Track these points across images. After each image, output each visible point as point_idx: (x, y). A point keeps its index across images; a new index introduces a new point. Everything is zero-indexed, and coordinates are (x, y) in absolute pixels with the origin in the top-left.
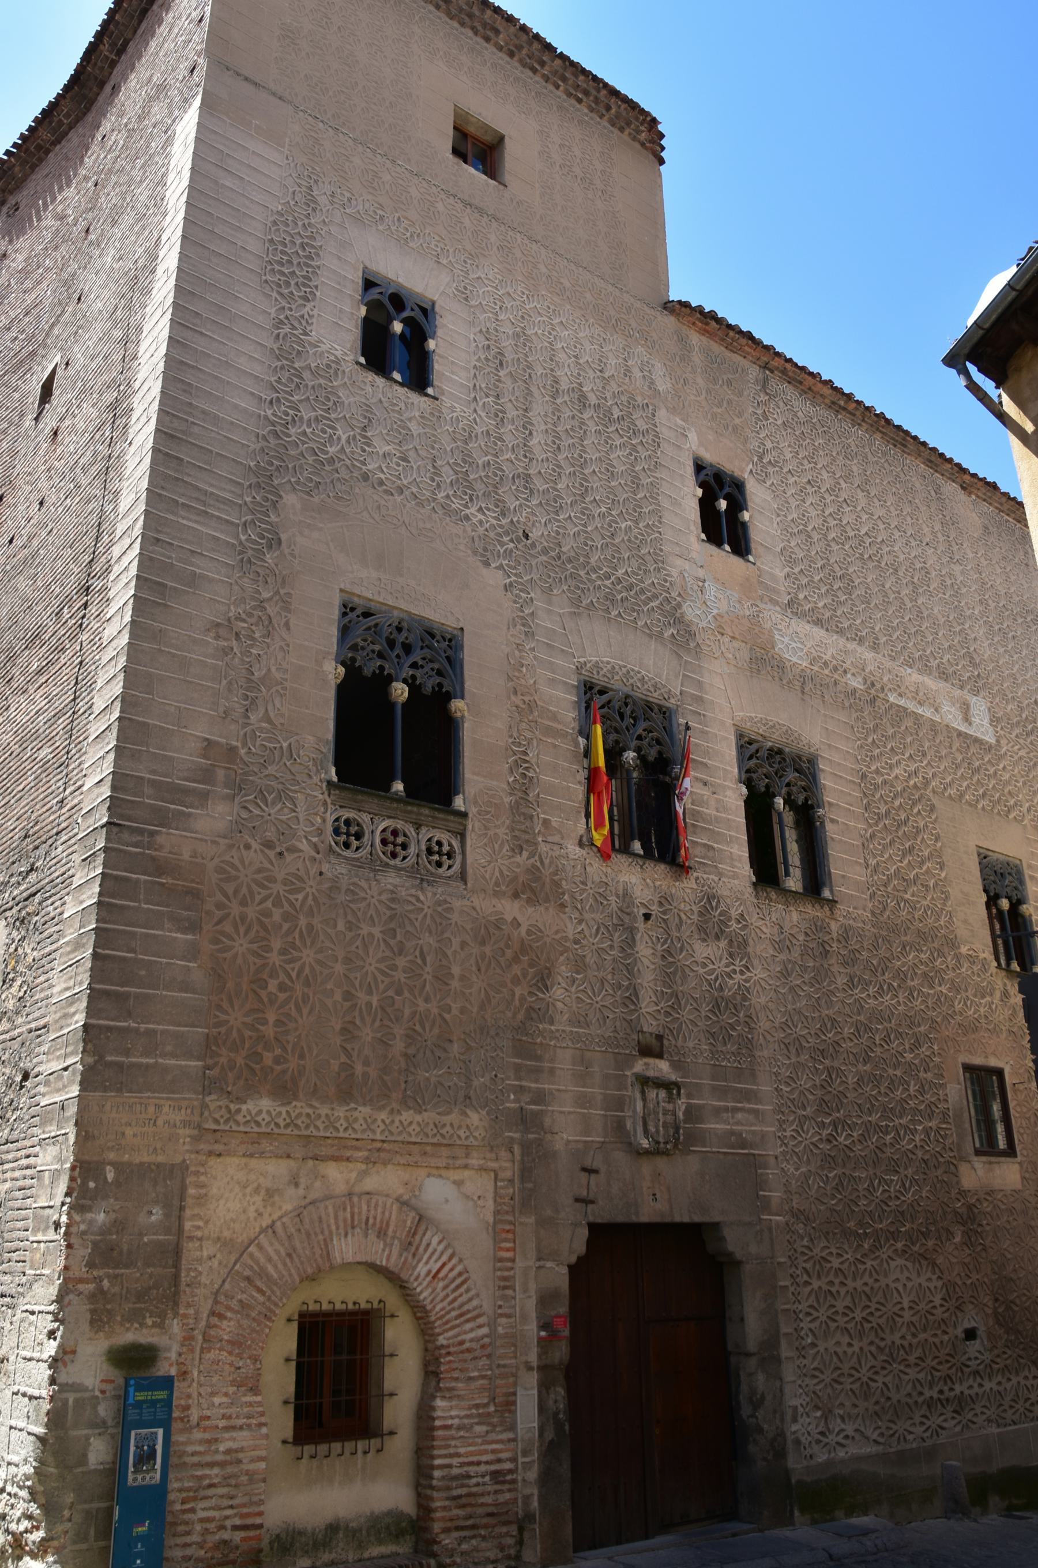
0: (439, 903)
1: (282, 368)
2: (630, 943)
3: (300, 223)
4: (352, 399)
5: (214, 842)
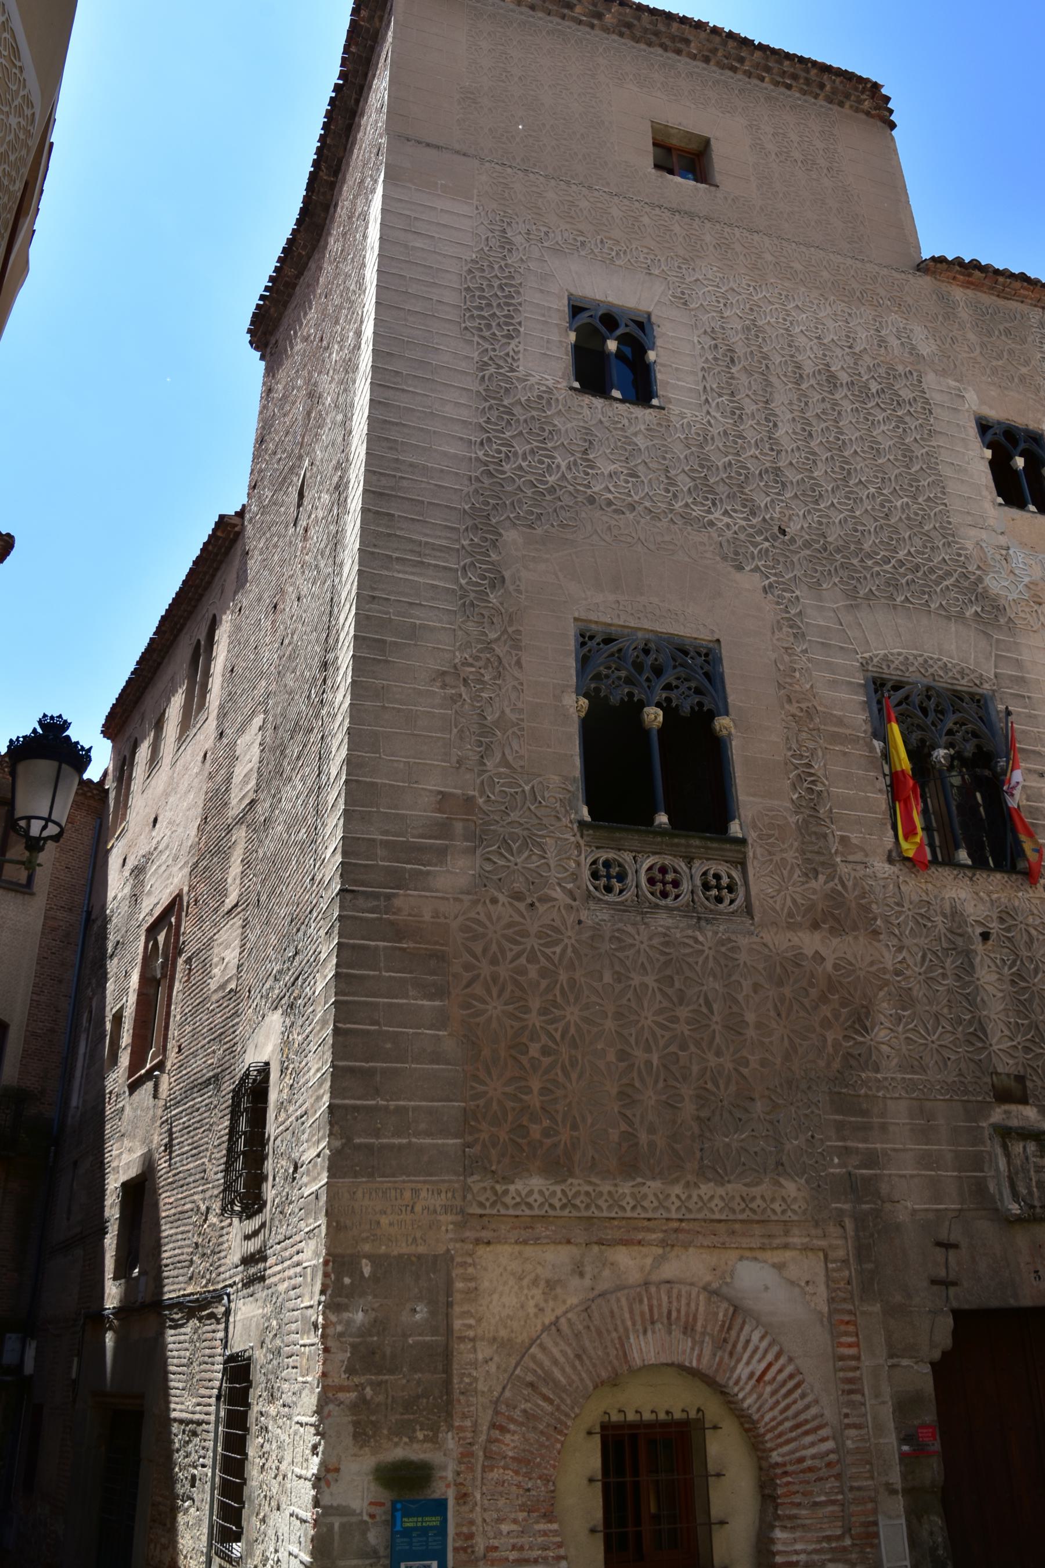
0: (722, 943)
1: (491, 408)
2: (968, 968)
3: (496, 267)
4: (569, 425)
5: (456, 899)
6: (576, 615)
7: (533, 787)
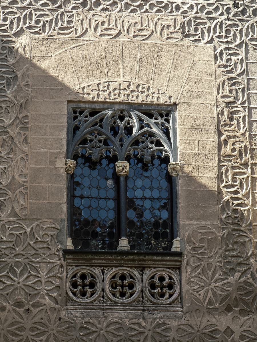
0: (158, 325)
6: (69, 98)
7: (32, 228)
